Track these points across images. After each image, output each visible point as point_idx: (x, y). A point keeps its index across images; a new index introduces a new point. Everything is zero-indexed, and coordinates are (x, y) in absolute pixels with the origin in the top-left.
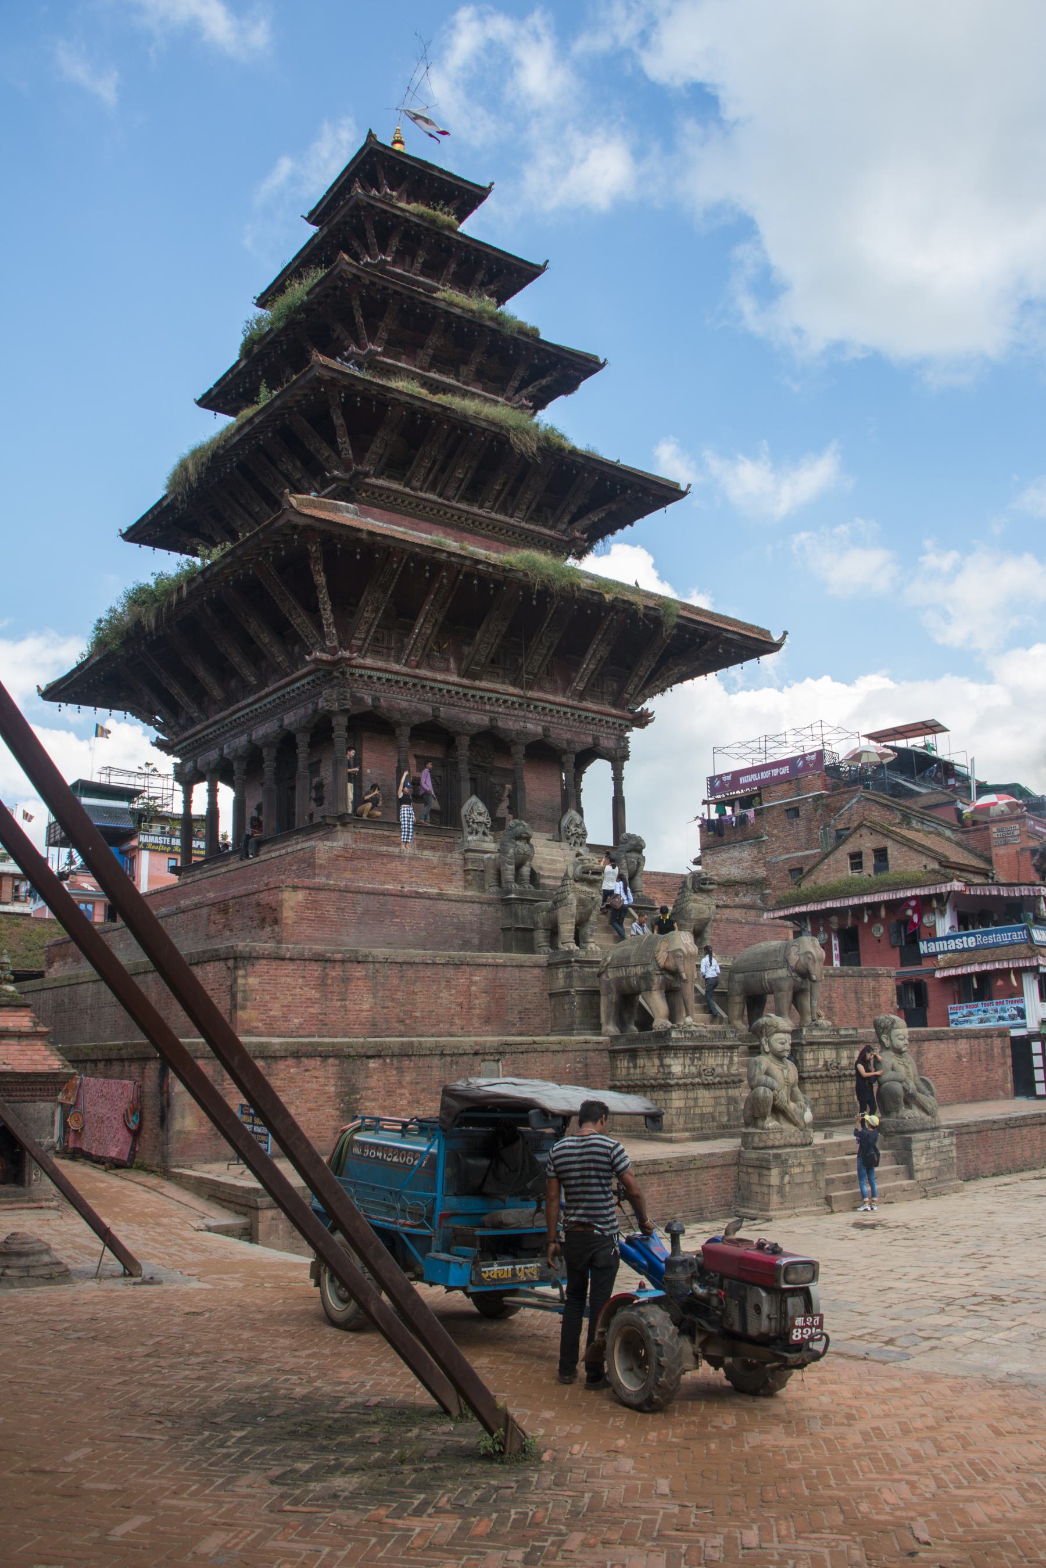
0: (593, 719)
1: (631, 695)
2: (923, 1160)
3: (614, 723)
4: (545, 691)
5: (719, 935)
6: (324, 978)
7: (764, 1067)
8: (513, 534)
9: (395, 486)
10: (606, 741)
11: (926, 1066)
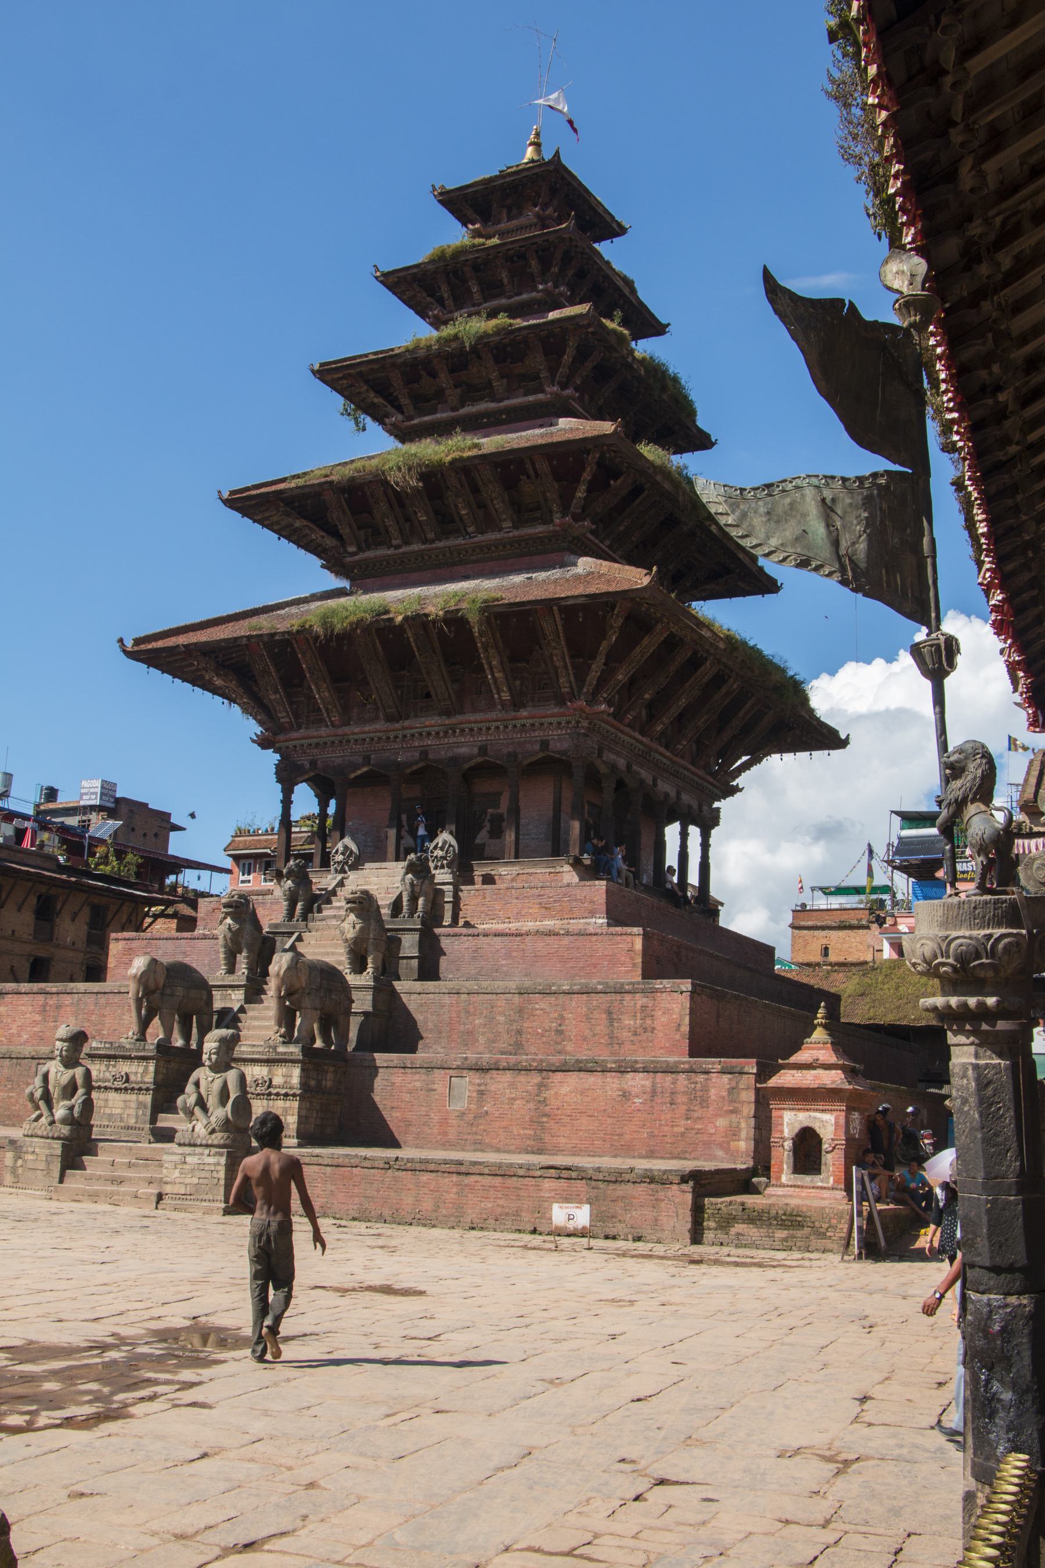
0: (533, 725)
1: (571, 687)
2: (177, 1173)
3: (559, 723)
4: (482, 711)
5: (523, 950)
6: (44, 1006)
7: (43, 1069)
8: (504, 547)
9: (382, 552)
10: (558, 744)
11: (554, 1103)
